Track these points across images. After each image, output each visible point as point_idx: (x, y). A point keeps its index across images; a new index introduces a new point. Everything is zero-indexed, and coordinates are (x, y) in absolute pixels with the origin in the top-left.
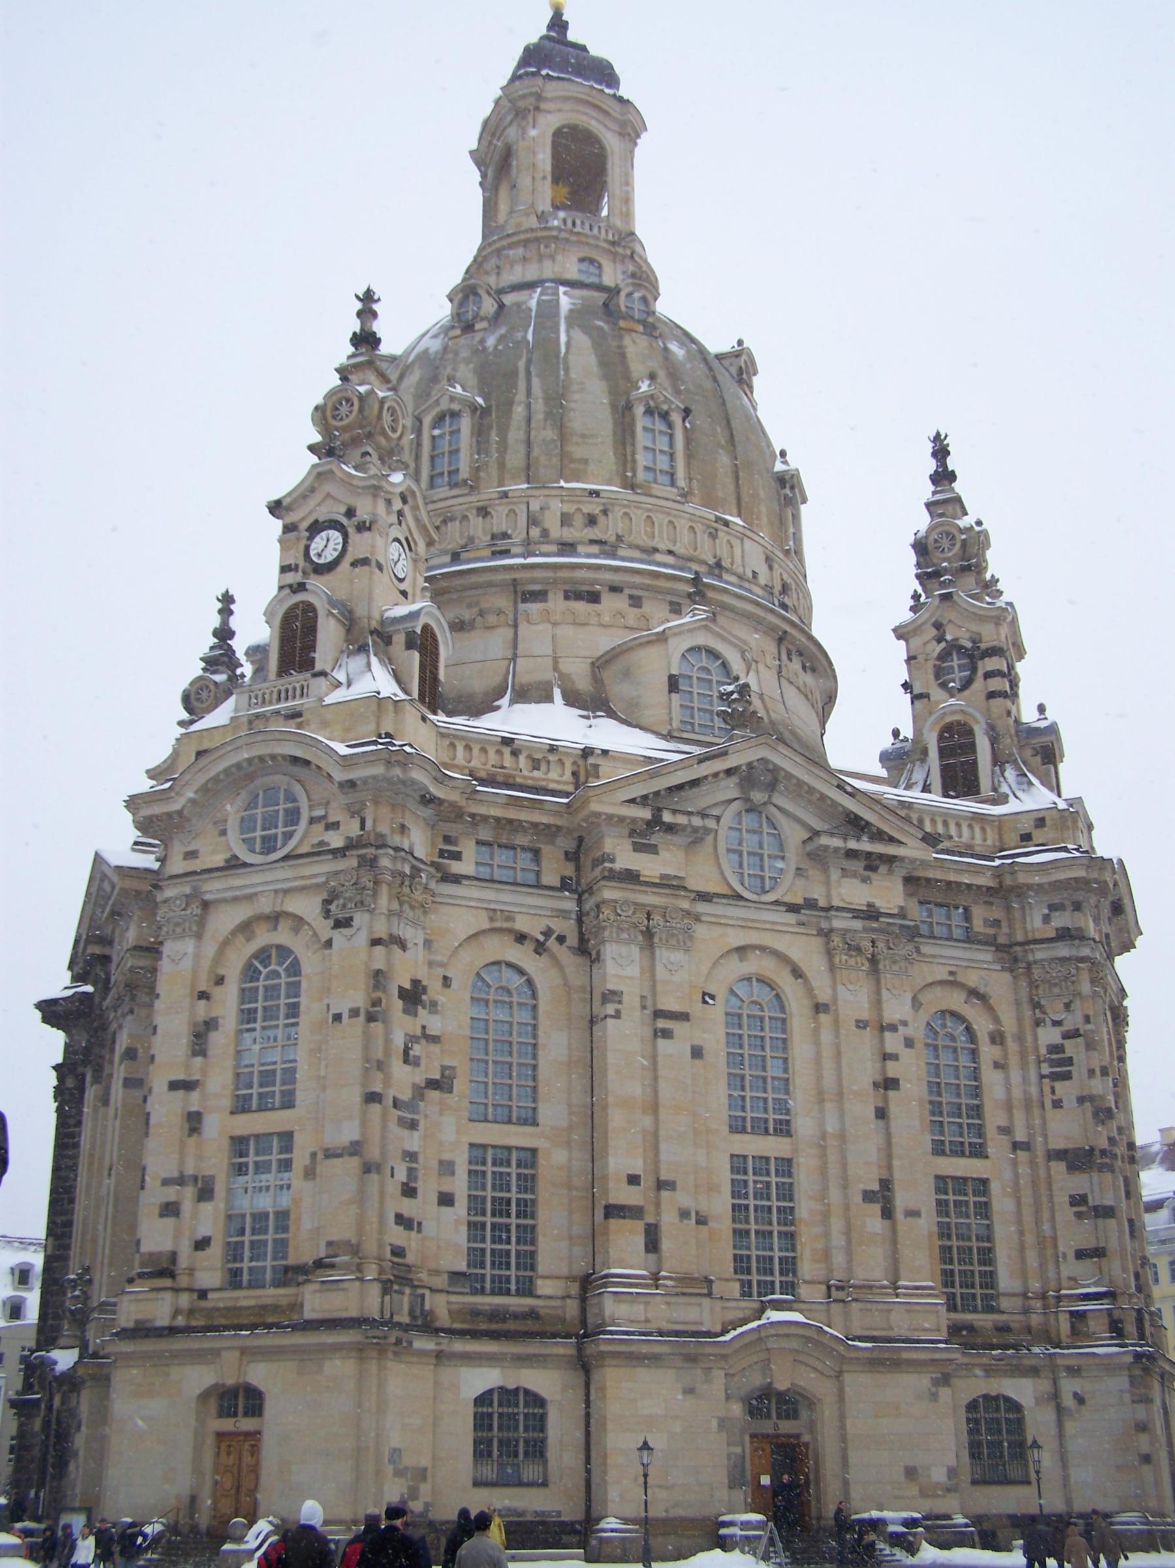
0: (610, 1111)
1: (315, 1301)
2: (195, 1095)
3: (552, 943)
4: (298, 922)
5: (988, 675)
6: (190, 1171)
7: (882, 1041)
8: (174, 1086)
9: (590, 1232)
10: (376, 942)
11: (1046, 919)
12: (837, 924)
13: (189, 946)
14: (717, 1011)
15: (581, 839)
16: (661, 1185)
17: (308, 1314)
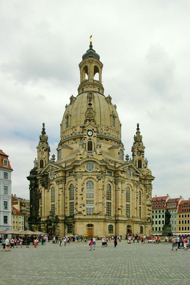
0: (119, 200)
1: (99, 217)
2: (82, 196)
3: (113, 182)
4: (93, 178)
5: (142, 155)
6: (82, 203)
7: (137, 194)
8: (80, 195)
9: (115, 211)
10: (103, 182)
11: (148, 182)
12: (135, 182)
13: (81, 180)
14: (125, 190)
15: (115, 172)
16: (122, 207)
17: (98, 218)
